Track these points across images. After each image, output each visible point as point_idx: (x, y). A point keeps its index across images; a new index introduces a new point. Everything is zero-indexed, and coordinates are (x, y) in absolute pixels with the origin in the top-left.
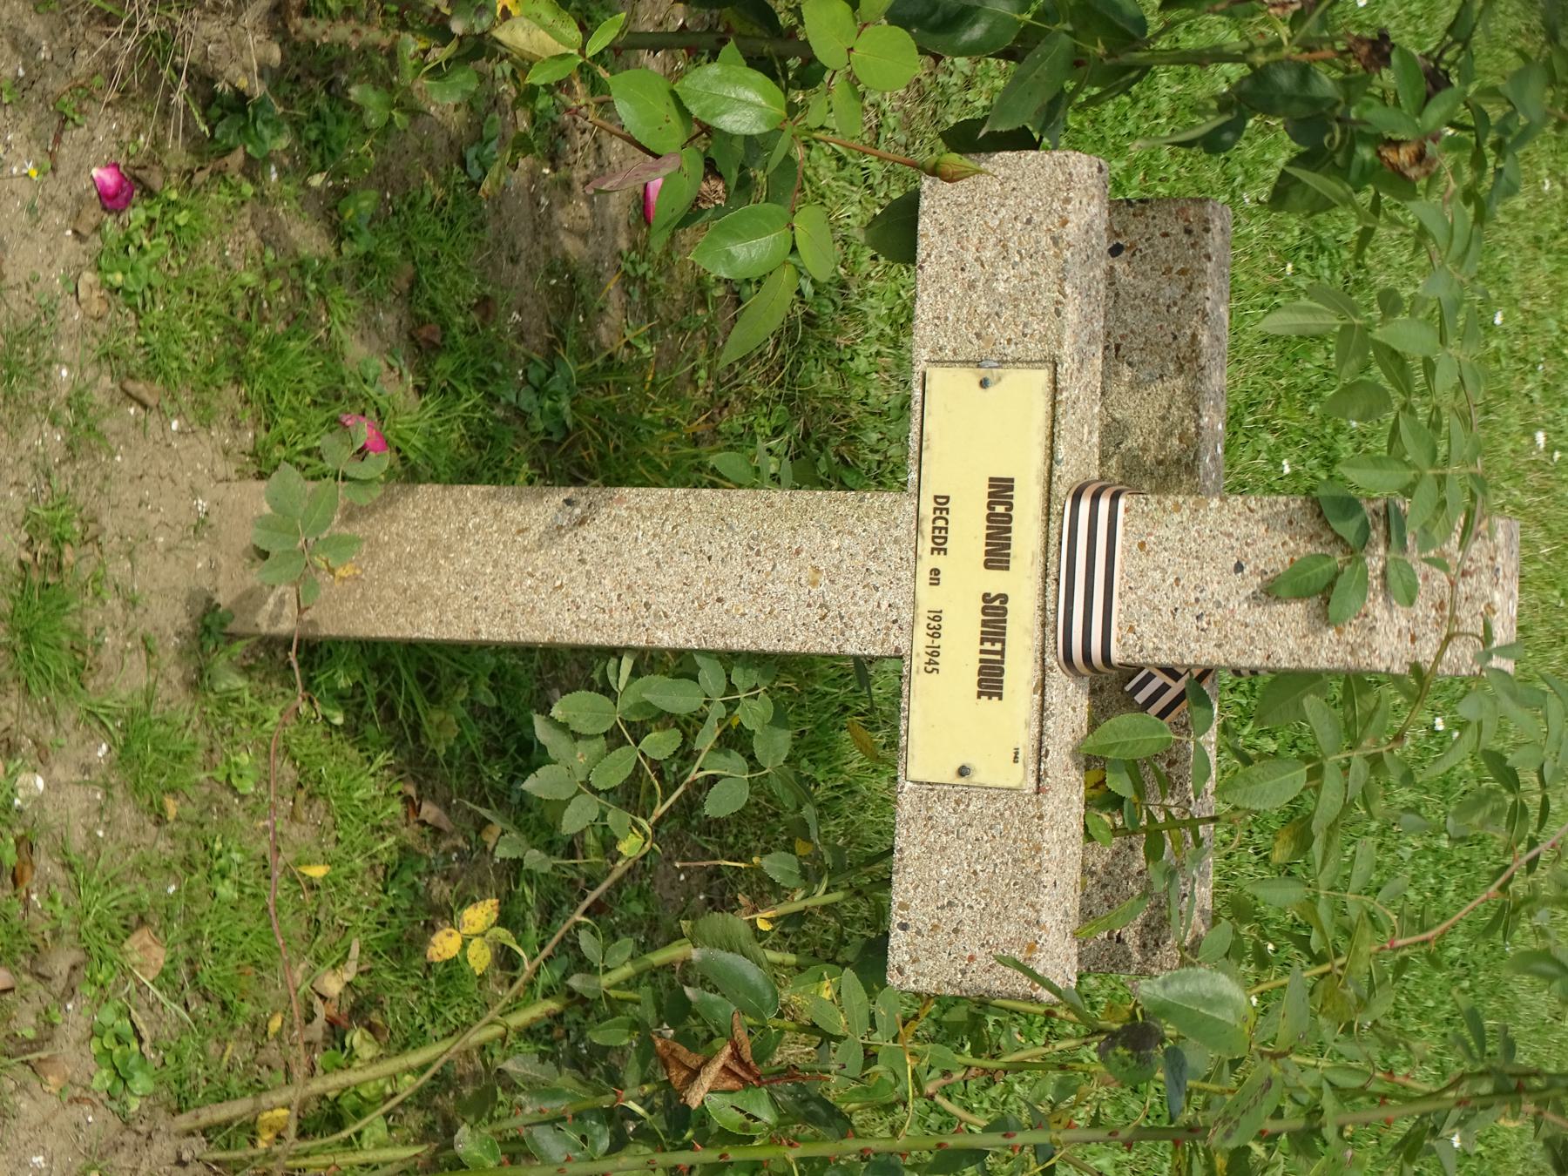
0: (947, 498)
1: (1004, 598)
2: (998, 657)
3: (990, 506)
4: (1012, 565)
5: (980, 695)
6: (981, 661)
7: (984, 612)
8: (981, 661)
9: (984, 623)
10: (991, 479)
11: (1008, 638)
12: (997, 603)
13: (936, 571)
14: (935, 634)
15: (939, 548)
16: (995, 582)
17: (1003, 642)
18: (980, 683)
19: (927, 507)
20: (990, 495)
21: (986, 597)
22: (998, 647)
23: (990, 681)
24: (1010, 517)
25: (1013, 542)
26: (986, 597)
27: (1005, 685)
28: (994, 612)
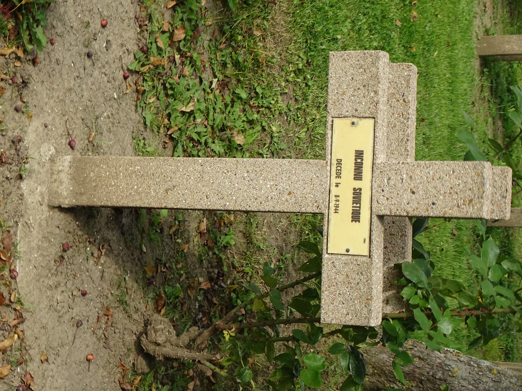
1: (360, 189)
2: (358, 209)
3: (356, 159)
5: (352, 221)
6: (353, 210)
8: (353, 210)
10: (356, 151)
11: (362, 202)
12: (358, 191)
16: (357, 184)
17: (360, 204)
18: (352, 217)
20: (356, 156)
21: (354, 189)
22: (358, 205)
23: (356, 217)
24: (362, 164)
25: (363, 171)
26: (354, 189)
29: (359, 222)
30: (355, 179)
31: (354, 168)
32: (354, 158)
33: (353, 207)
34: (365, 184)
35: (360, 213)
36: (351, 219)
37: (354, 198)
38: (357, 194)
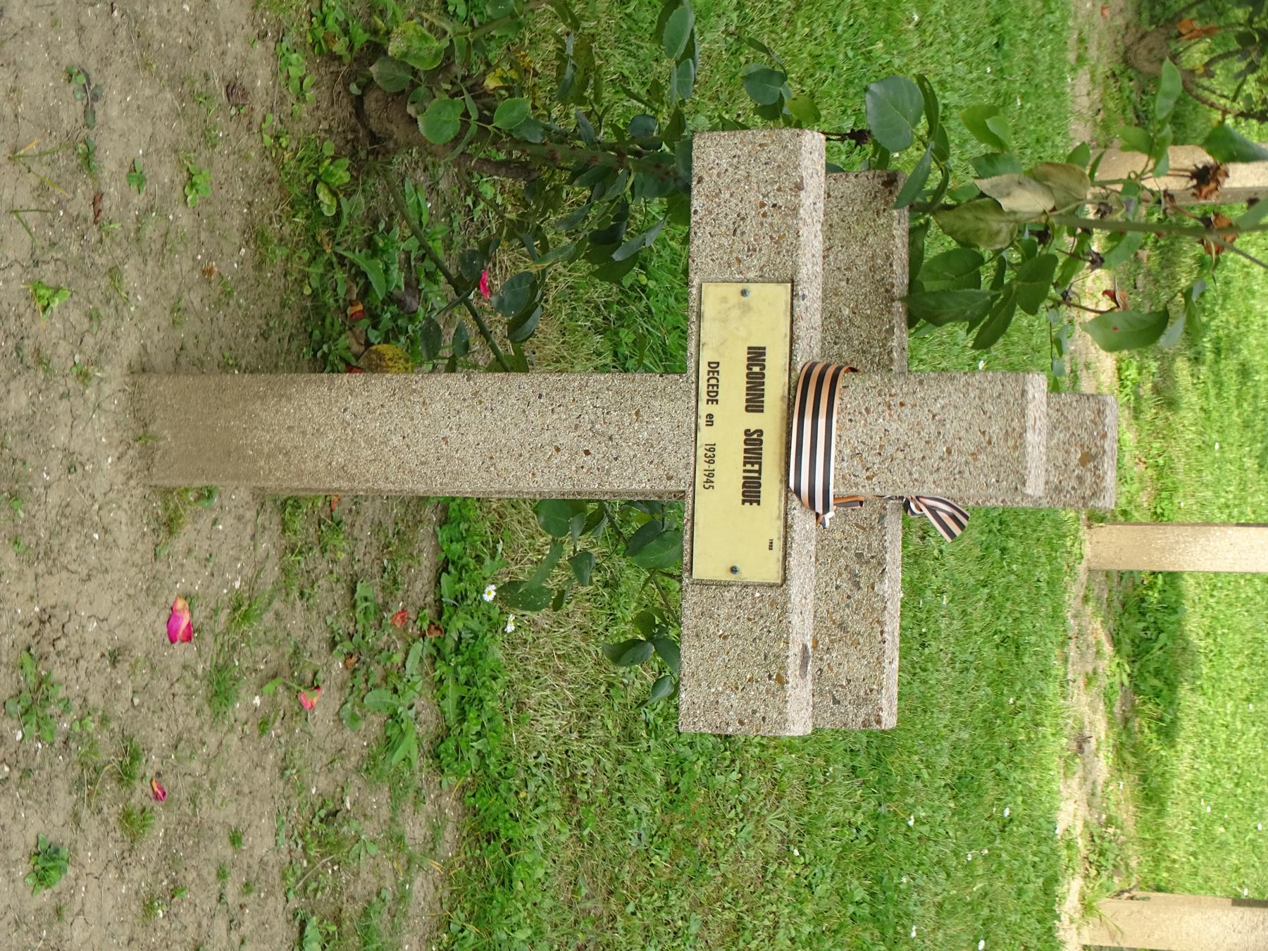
1: (760, 432)
3: (749, 367)
4: (765, 409)
5: (744, 502)
7: (746, 442)
9: (746, 451)
13: (710, 416)
14: (711, 461)
16: (755, 421)
17: (760, 464)
18: (743, 493)
19: (704, 369)
20: (749, 359)
21: (747, 432)
22: (756, 467)
23: (751, 492)
24: (763, 376)
26: (747, 432)
31: (745, 385)
33: (745, 471)
34: (769, 421)
38: (753, 442)
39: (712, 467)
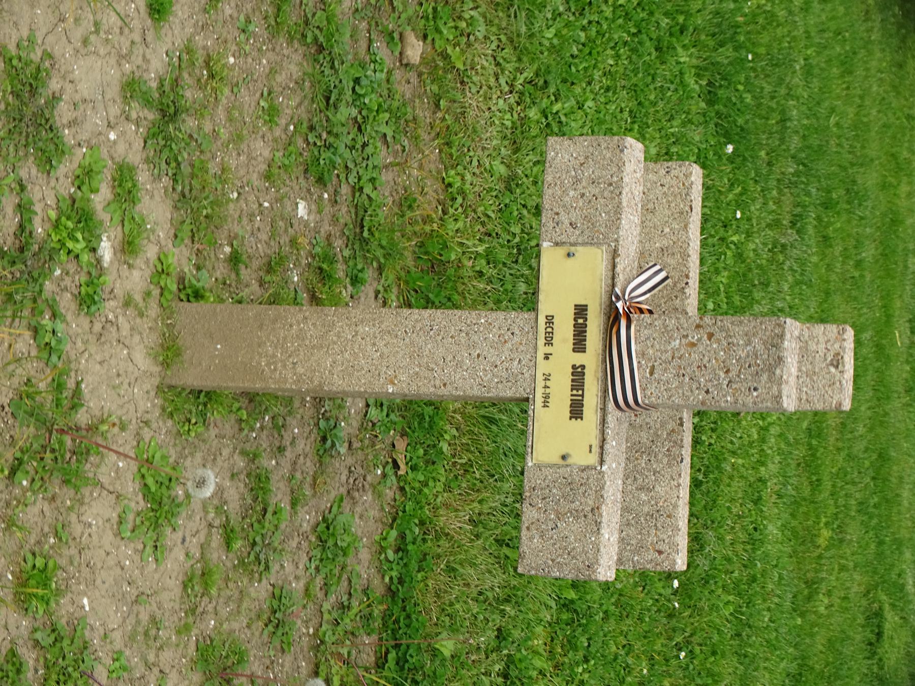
0: (553, 317)
1: (583, 367)
3: (575, 320)
5: (571, 418)
10: (576, 306)
11: (586, 388)
12: (579, 370)
15: (549, 342)
16: (579, 359)
17: (583, 390)
19: (542, 320)
20: (575, 314)
21: (574, 367)
22: (580, 392)
23: (576, 411)
25: (587, 338)
27: (584, 412)
28: (578, 373)
29: (582, 419)
30: (574, 350)
31: (572, 333)
32: (573, 316)
33: (572, 395)
34: (591, 359)
35: (582, 405)
36: (569, 415)
37: (573, 381)
39: (548, 391)
